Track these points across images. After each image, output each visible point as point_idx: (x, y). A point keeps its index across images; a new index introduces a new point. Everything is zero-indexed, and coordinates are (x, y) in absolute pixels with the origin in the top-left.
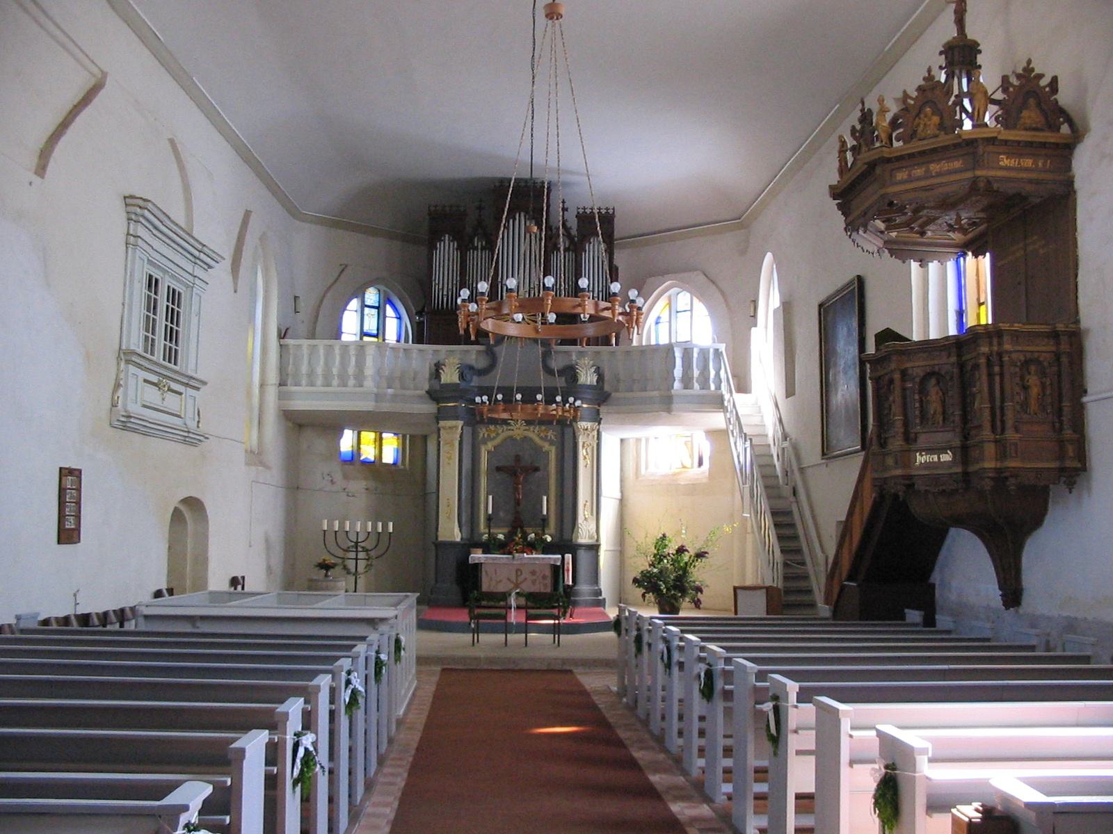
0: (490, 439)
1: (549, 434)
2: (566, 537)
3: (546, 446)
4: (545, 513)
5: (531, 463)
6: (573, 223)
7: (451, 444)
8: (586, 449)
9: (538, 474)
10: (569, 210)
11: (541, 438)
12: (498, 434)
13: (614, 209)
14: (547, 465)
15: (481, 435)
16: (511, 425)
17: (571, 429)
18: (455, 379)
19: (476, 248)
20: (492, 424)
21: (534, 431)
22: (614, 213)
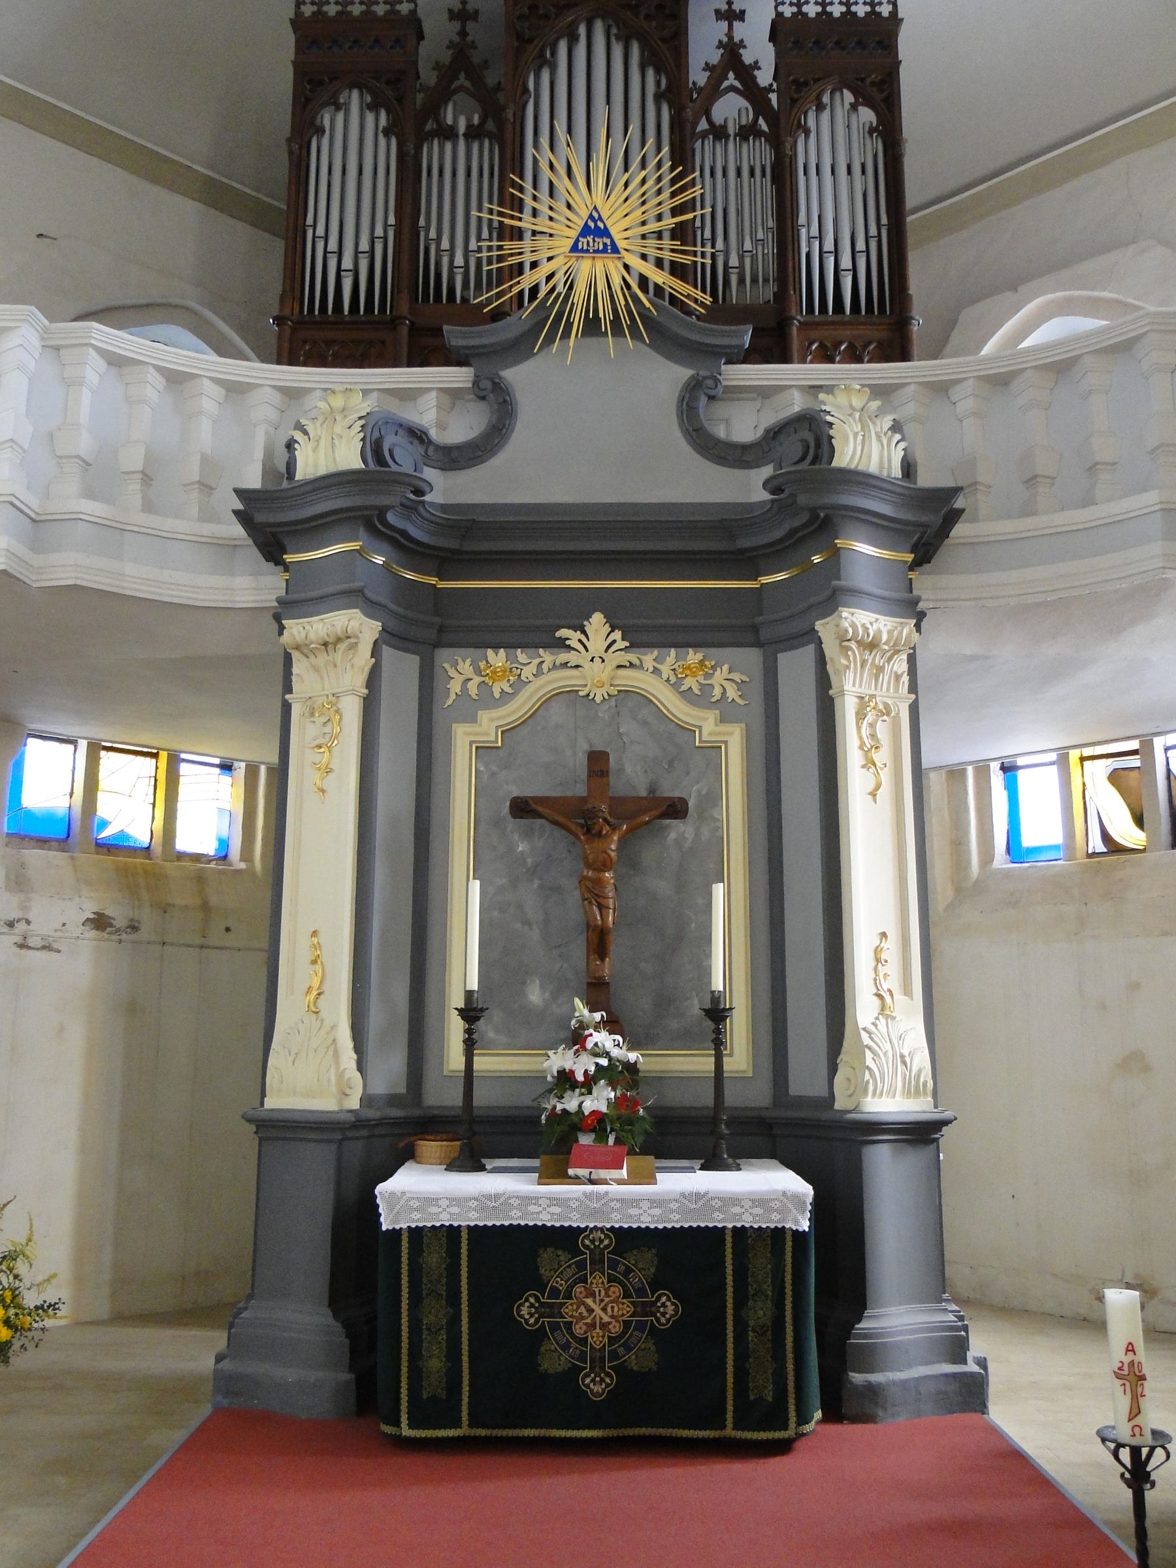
0: (487, 700)
1: (720, 676)
3: (708, 726)
4: (718, 984)
5: (652, 790)
8: (872, 725)
9: (677, 830)
11: (687, 695)
12: (519, 684)
14: (713, 798)
15: (455, 687)
17: (811, 649)
19: (449, 134)
20: (496, 647)
21: (656, 671)
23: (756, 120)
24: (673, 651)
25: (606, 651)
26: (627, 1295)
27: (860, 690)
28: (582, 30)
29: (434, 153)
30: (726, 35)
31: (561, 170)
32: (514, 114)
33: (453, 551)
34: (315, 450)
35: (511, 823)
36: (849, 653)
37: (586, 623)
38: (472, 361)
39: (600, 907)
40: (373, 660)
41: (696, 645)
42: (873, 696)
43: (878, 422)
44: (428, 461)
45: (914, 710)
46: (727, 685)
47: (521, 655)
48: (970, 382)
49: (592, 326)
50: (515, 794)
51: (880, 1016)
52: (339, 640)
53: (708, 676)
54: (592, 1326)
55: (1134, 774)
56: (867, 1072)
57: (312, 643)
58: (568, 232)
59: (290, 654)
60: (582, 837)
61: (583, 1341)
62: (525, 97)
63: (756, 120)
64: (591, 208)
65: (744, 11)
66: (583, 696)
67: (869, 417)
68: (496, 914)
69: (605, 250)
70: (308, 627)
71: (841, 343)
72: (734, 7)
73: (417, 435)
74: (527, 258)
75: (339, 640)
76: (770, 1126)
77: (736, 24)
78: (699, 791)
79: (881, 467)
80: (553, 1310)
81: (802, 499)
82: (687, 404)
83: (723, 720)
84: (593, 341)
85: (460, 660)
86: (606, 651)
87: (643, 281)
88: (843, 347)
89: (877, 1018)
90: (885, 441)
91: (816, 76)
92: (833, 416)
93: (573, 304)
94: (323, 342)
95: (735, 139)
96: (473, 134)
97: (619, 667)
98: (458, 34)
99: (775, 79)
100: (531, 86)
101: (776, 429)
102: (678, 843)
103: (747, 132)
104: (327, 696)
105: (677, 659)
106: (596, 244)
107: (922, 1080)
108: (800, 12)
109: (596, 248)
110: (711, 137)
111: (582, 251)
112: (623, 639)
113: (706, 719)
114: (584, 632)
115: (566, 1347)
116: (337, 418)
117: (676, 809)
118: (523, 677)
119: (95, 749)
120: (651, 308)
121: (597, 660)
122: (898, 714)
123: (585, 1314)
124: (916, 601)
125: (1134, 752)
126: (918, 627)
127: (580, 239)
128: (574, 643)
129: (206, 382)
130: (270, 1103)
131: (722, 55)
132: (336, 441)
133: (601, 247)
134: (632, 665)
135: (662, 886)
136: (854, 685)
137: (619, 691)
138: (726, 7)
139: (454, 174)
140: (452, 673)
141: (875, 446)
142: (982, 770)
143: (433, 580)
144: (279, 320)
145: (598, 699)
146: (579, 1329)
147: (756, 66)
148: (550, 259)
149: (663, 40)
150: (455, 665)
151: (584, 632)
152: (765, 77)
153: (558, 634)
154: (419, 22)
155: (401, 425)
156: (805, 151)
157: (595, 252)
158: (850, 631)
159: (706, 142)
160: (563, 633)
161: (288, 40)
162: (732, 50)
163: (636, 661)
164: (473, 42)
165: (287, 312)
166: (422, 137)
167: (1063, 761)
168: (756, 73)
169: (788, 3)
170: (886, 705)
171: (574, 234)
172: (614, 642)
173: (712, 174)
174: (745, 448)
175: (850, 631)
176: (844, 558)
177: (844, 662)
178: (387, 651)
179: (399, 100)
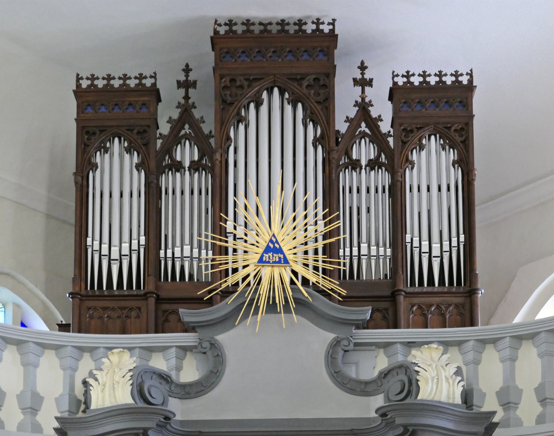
10: (374, 83)
13: (471, 76)
19: (178, 167)
22: (471, 81)
72: (365, 76)
77: (367, 89)
88: (433, 309)
91: (419, 126)
96: (195, 167)
98: (183, 98)
99: (392, 127)
103: (373, 164)
108: (409, 82)
131: (358, 111)
139: (182, 193)
147: (380, 119)
149: (319, 103)
152: (385, 127)
159: (347, 170)
165: (77, 289)
166: (161, 171)
179: (146, 145)
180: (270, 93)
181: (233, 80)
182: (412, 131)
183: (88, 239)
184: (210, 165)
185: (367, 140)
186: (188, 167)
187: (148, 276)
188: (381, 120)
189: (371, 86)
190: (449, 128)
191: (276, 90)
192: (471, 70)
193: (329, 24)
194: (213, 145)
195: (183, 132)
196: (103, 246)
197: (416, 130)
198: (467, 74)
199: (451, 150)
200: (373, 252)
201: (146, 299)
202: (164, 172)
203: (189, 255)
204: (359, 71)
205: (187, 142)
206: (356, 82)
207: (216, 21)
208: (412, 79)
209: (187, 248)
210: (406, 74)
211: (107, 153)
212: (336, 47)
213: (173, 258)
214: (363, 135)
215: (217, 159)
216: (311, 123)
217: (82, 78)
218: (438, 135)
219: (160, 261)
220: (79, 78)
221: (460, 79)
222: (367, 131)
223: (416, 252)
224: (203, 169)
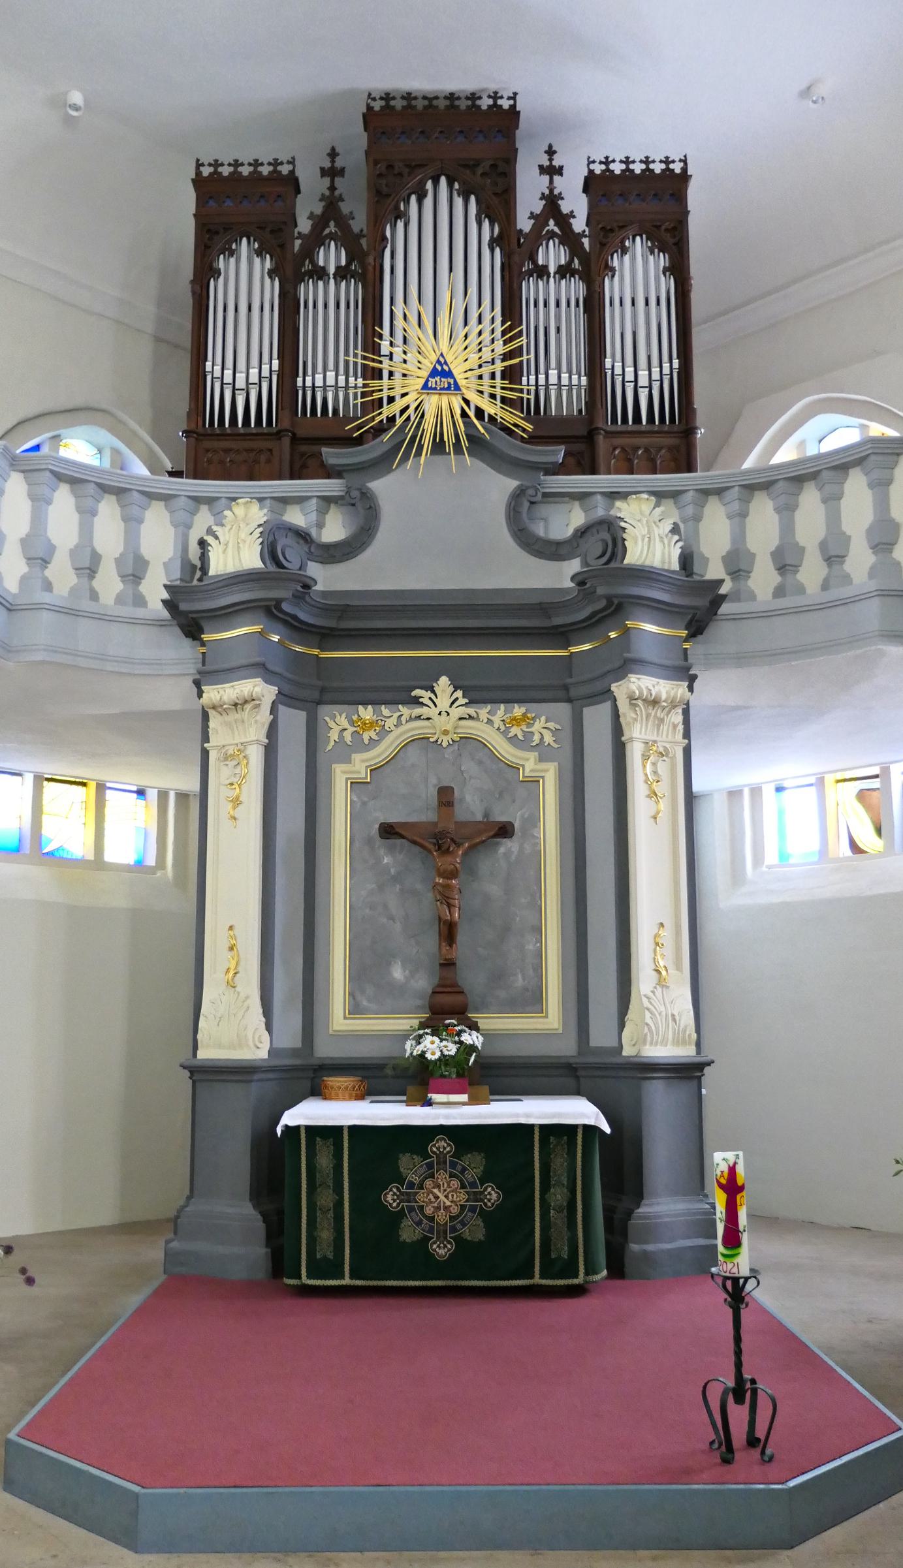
0: (359, 745)
1: (538, 726)
2: (600, 1037)
3: (530, 764)
5: (486, 815)
6: (576, 205)
7: (235, 757)
8: (654, 764)
9: (508, 846)
10: (565, 171)
11: (513, 740)
12: (384, 733)
13: (686, 164)
14: (533, 821)
15: (334, 736)
16: (422, 704)
17: (607, 706)
18: (251, 558)
19: (320, 273)
20: (365, 703)
21: (490, 722)
22: (685, 169)
23: (571, 261)
24: (502, 706)
25: (450, 707)
26: (463, 1187)
27: (646, 737)
28: (429, 185)
29: (309, 291)
30: (548, 187)
31: (413, 319)
32: (375, 260)
33: (331, 629)
34: (224, 551)
35: (378, 841)
36: (637, 709)
37: (435, 685)
38: (345, 475)
39: (450, 906)
40: (272, 716)
41: (520, 701)
42: (655, 742)
43: (661, 525)
44: (312, 557)
45: (687, 752)
46: (544, 732)
47: (385, 711)
48: (737, 488)
49: (439, 447)
50: (382, 820)
51: (658, 987)
52: (246, 702)
53: (529, 725)
54: (438, 1208)
55: (875, 794)
56: (646, 1028)
57: (225, 704)
58: (420, 373)
59: (207, 712)
60: (435, 853)
61: (432, 1219)
62: (385, 243)
63: (571, 261)
64: (439, 354)
65: (563, 166)
66: (433, 742)
67: (655, 523)
68: (367, 911)
69: (449, 388)
70: (222, 692)
71: (639, 448)
73: (302, 536)
74: (385, 394)
75: (246, 702)
76: (576, 1069)
78: (522, 816)
79: (663, 562)
80: (410, 1198)
81: (600, 591)
82: (514, 509)
83: (541, 759)
84: (438, 458)
85: (337, 714)
86: (450, 707)
87: (480, 413)
88: (640, 452)
89: (655, 988)
90: (666, 542)
91: (621, 225)
92: (625, 522)
93: (423, 430)
94: (222, 451)
95: (554, 277)
96: (342, 273)
97: (461, 719)
98: (328, 188)
99: (587, 225)
100: (388, 233)
101: (583, 530)
102: (507, 855)
103: (564, 271)
104: (237, 744)
105: (506, 712)
106: (442, 383)
107: (688, 1033)
108: (608, 170)
109: (442, 386)
110: (535, 275)
111: (431, 388)
112: (464, 697)
113: (528, 760)
114: (433, 692)
115: (419, 1223)
116: (241, 525)
117: (505, 831)
118: (386, 728)
119: (39, 780)
120: (485, 434)
121: (444, 714)
122: (675, 755)
123: (433, 1200)
124: (689, 669)
125: (876, 776)
126: (691, 689)
127: (430, 379)
128: (425, 701)
129: (135, 494)
130: (202, 1054)
131: (545, 206)
132: (241, 545)
133: (446, 386)
134: (471, 717)
135: (494, 889)
136: (641, 733)
137: (460, 738)
138: (548, 163)
139: (326, 306)
140: (332, 724)
141: (658, 546)
142: (756, 791)
143: (316, 652)
144: (187, 433)
145: (445, 744)
146: (429, 1210)
148: (403, 395)
149: (496, 194)
150: (333, 718)
151: (433, 692)
152: (579, 224)
153: (413, 694)
154: (297, 180)
155: (290, 529)
156: (611, 288)
157: (441, 389)
158: (637, 692)
159: (531, 278)
160: (416, 693)
161: (188, 199)
162: (552, 201)
163: (474, 714)
164: (341, 195)
165: (193, 426)
166: (300, 278)
167: (820, 782)
168: (572, 220)
169: (598, 161)
170: (665, 748)
171: (425, 374)
172: (457, 699)
173: (536, 305)
174: (558, 544)
175: (637, 692)
176: (633, 633)
177: (634, 716)
178: (281, 707)
179: (282, 246)
180: (436, 183)
181: (390, 167)
182: (612, 230)
183: (207, 363)
184: (360, 271)
185: (557, 241)
186: (334, 274)
187: (282, 409)
188: (574, 217)
189: (561, 175)
190: (658, 227)
191: (443, 180)
192: (685, 156)
193: (509, 98)
194: (365, 247)
195: (327, 231)
196: (225, 372)
197: (617, 229)
198: (681, 160)
199: (661, 254)
200: (565, 381)
201: (280, 439)
202: (303, 280)
203: (333, 383)
204: (546, 157)
205: (333, 243)
206: (543, 170)
207: (370, 94)
208: (612, 166)
209: (331, 375)
210: (604, 160)
211: (232, 256)
212: (517, 127)
213: (314, 387)
214: (552, 235)
215: (369, 264)
216: (487, 220)
217: (203, 165)
218: (644, 236)
219: (297, 391)
220: (199, 165)
221: (672, 166)
222: (556, 230)
223: (619, 380)
224: (352, 276)
